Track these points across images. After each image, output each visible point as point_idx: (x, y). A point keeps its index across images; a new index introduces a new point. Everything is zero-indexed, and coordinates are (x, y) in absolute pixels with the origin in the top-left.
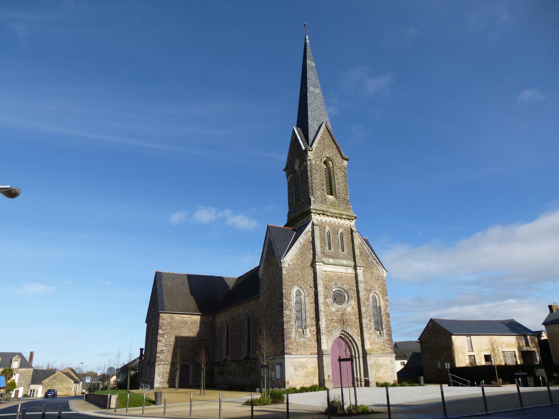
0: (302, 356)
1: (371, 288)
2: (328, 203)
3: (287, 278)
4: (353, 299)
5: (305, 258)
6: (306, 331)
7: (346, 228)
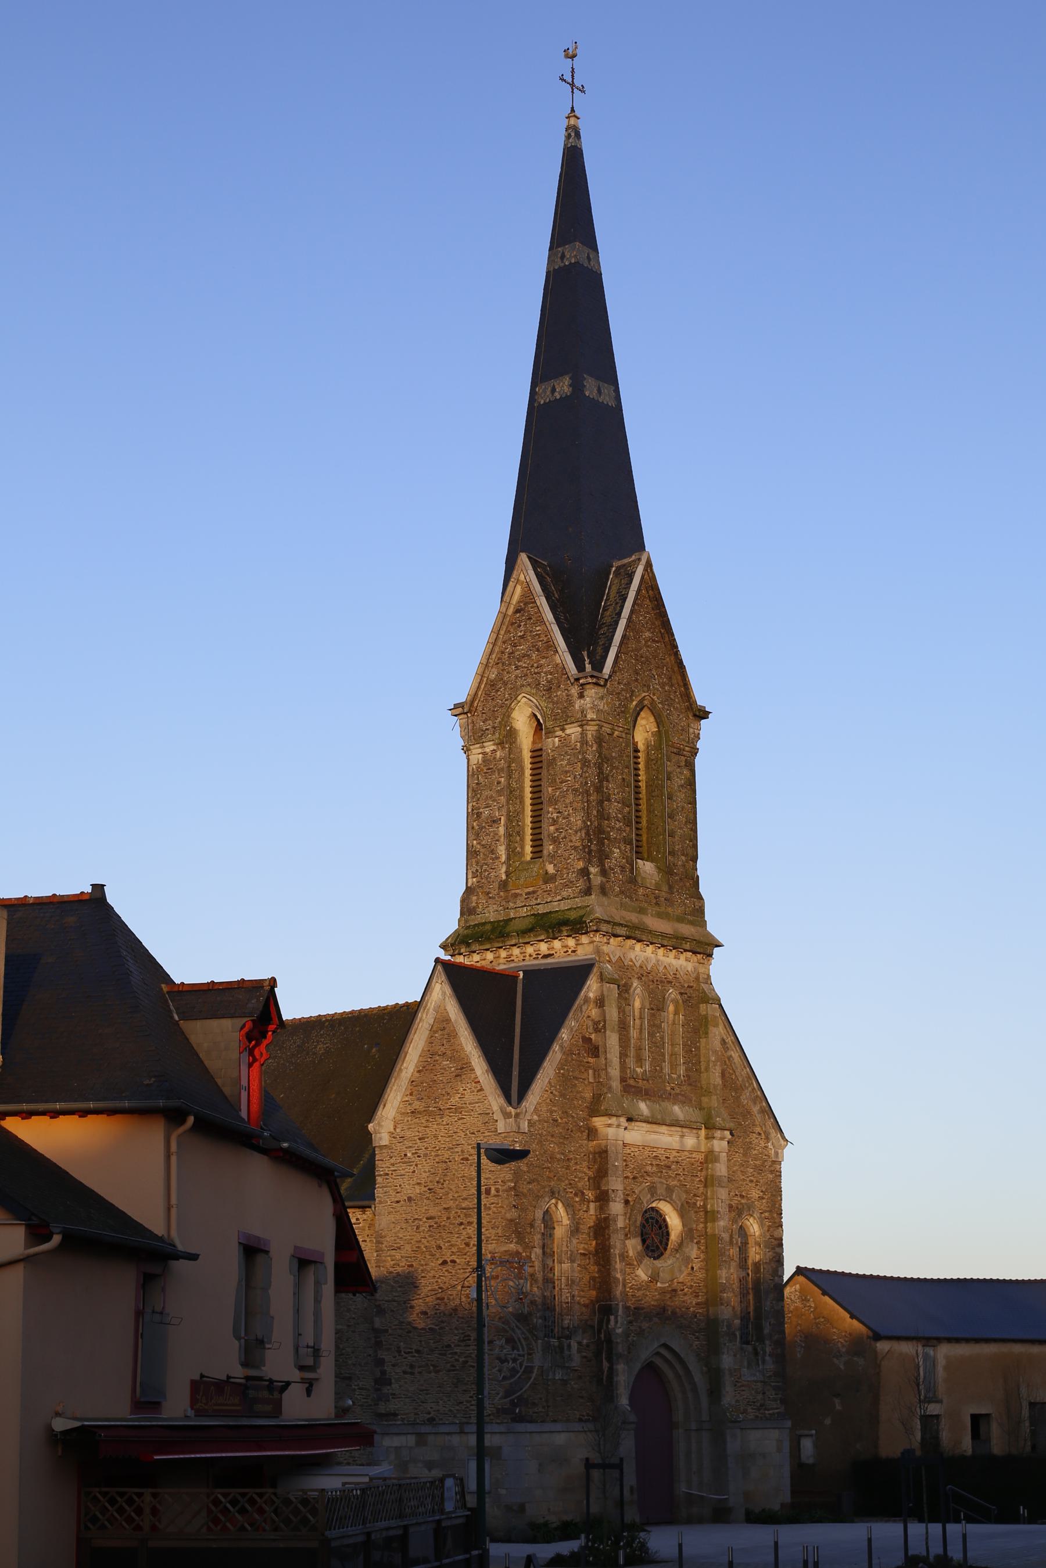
0: (558, 1427)
1: (739, 1199)
2: (641, 891)
3: (525, 1169)
4: (695, 1241)
5: (572, 1100)
6: (569, 1346)
7: (686, 985)
